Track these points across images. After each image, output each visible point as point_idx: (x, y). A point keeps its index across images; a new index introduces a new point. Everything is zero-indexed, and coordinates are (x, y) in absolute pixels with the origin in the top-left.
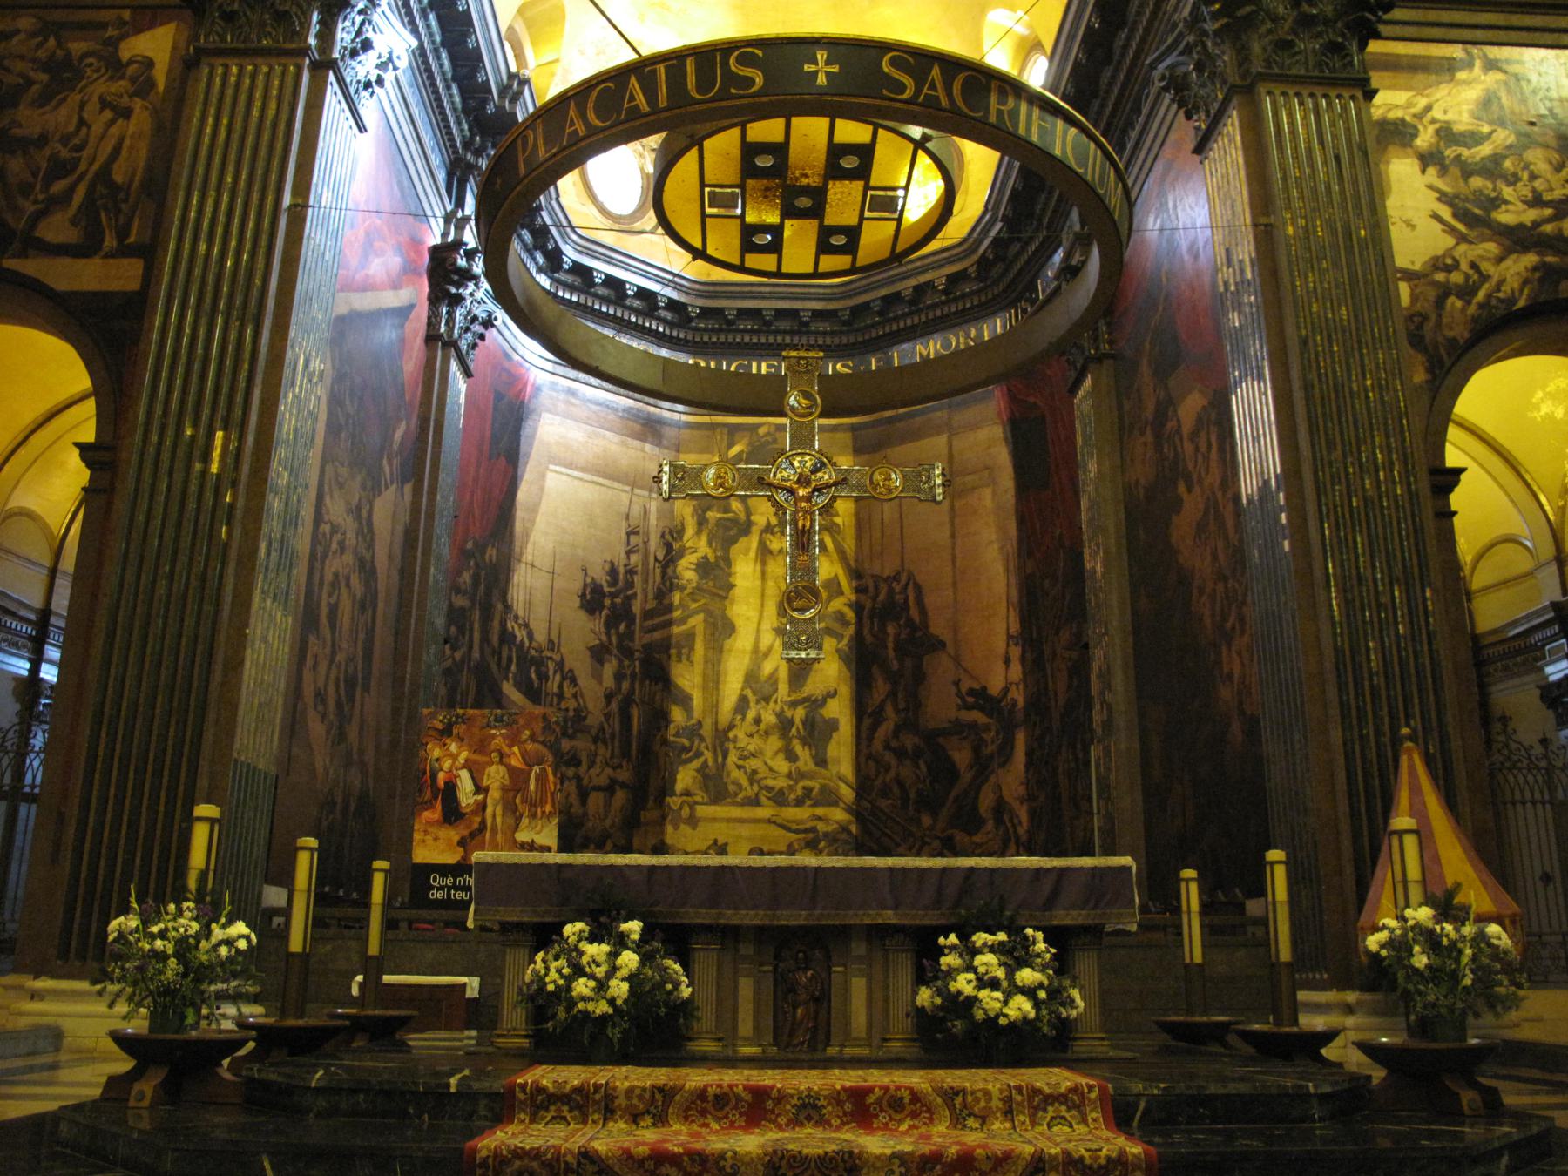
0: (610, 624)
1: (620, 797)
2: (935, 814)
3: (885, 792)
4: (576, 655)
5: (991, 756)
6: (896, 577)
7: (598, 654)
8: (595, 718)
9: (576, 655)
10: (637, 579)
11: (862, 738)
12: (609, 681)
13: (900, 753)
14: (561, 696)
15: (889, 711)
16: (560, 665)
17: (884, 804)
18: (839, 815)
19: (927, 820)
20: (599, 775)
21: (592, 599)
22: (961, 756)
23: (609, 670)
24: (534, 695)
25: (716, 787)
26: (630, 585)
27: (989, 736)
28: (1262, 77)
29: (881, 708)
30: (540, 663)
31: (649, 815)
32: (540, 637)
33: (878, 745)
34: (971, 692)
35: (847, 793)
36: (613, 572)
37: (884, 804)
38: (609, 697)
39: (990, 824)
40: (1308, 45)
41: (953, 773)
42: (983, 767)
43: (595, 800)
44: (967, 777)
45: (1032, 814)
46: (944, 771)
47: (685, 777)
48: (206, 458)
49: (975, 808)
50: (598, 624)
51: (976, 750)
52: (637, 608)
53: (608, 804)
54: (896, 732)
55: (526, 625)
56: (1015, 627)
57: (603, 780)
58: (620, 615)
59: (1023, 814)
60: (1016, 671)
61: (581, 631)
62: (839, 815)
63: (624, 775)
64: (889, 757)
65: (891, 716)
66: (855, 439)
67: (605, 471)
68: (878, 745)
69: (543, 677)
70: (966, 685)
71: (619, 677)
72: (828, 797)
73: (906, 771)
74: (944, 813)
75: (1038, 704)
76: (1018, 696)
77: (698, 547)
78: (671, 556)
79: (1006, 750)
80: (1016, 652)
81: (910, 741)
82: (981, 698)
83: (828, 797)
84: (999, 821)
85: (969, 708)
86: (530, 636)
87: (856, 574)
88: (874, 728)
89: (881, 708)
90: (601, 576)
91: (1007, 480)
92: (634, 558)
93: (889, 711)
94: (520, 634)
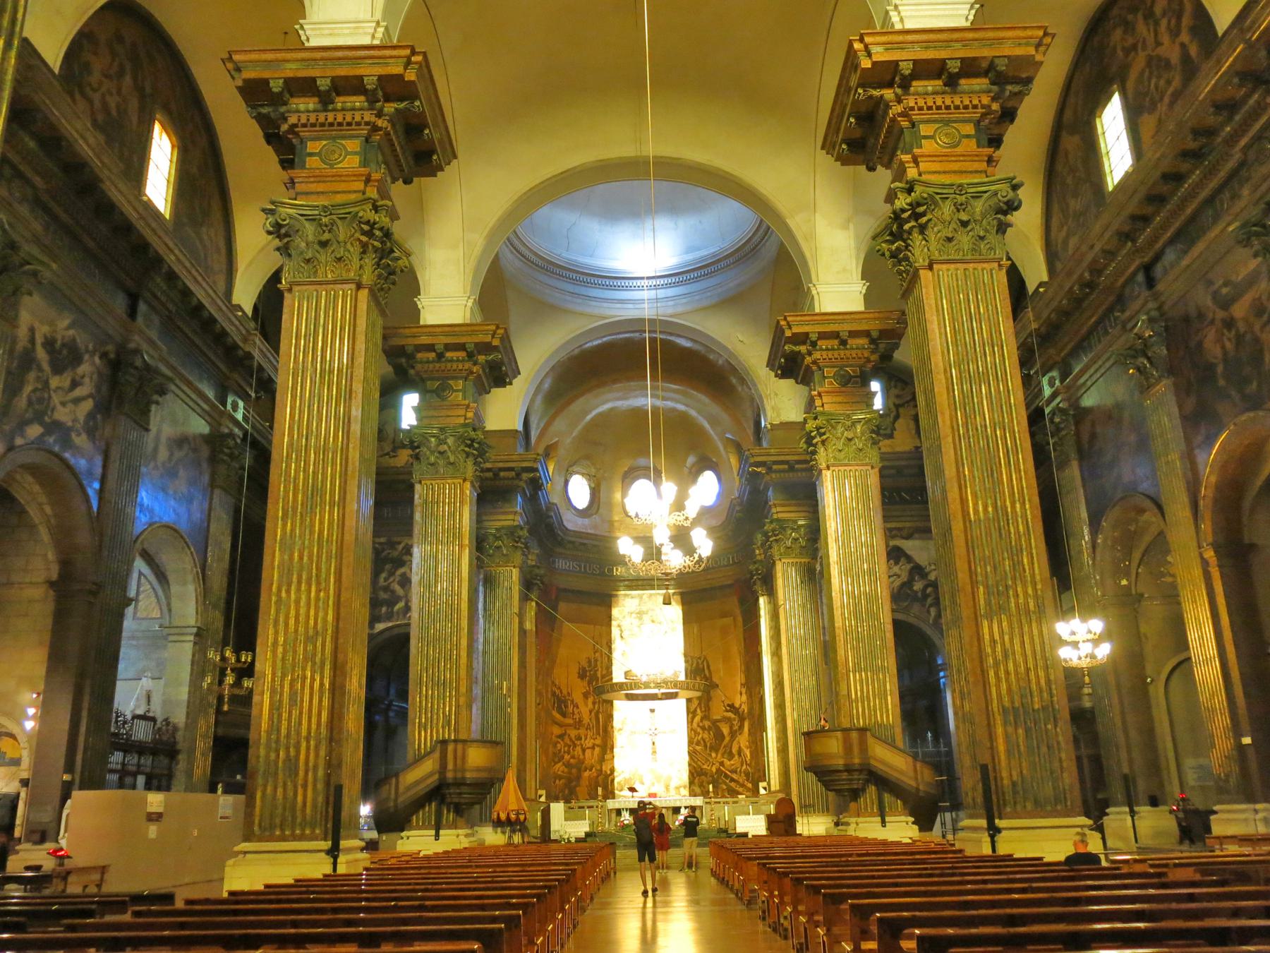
0: (590, 683)
1: (597, 750)
2: (717, 752)
3: (698, 743)
5: (736, 731)
6: (700, 658)
8: (586, 720)
10: (599, 663)
12: (590, 706)
13: (703, 728)
14: (573, 713)
15: (698, 710)
16: (572, 701)
17: (698, 748)
19: (714, 755)
20: (589, 743)
22: (726, 730)
23: (590, 700)
24: (564, 715)
26: (596, 666)
27: (735, 723)
29: (696, 710)
30: (565, 702)
31: (607, 757)
32: (565, 692)
33: (695, 725)
34: (728, 705)
36: (589, 662)
37: (698, 748)
38: (591, 712)
39: (736, 757)
40: (965, 240)
41: (723, 737)
42: (733, 734)
43: (588, 752)
44: (727, 739)
45: (751, 753)
46: (719, 736)
48: (502, 688)
49: (731, 751)
50: (585, 683)
51: (731, 728)
52: (599, 675)
53: (593, 754)
54: (702, 720)
55: (559, 688)
56: (743, 681)
57: (590, 745)
58: (594, 678)
59: (748, 752)
60: (744, 698)
63: (598, 741)
64: (699, 730)
66: (682, 599)
68: (695, 725)
69: (566, 707)
70: (727, 702)
71: (594, 703)
73: (706, 736)
74: (721, 752)
75: (751, 709)
76: (745, 708)
79: (741, 727)
80: (744, 690)
81: (707, 723)
84: (740, 755)
85: (727, 711)
86: (561, 692)
88: (693, 719)
89: (696, 710)
92: (597, 654)
93: (698, 710)
94: (557, 692)
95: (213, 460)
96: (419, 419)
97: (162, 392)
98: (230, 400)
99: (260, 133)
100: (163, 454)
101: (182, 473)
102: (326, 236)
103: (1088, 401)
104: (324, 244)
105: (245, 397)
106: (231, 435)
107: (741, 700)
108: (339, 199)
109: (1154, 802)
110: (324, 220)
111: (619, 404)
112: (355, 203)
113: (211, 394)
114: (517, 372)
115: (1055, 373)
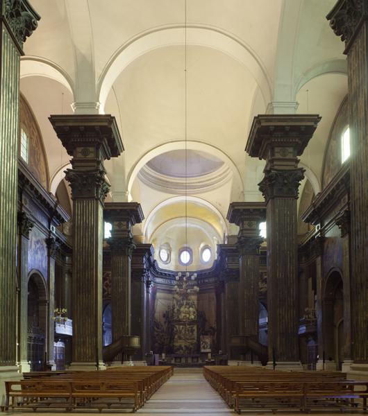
4: (162, 323)
7: (165, 322)
9: (162, 323)
11: (198, 332)
18: (195, 341)
21: (164, 316)
23: (167, 324)
24: (158, 328)
25: (180, 338)
28: (276, 197)
35: (196, 338)
47: (176, 337)
61: (163, 320)
62: (195, 341)
65: (201, 329)
67: (165, 299)
72: (194, 339)
76: (216, 328)
77: (177, 307)
78: (174, 309)
82: (211, 328)
83: (194, 339)
87: (197, 311)
90: (165, 312)
91: (215, 299)
95: (49, 247)
96: (112, 235)
97: (32, 226)
98: (51, 227)
99: (66, 151)
100: (33, 246)
101: (39, 252)
102: (85, 182)
103: (327, 235)
104: (85, 185)
105: (56, 225)
106: (53, 239)
107: (214, 325)
108: (89, 169)
109: (330, 359)
110: (84, 176)
111: (178, 225)
112: (94, 171)
113: (45, 224)
114: (144, 218)
115: (319, 225)
